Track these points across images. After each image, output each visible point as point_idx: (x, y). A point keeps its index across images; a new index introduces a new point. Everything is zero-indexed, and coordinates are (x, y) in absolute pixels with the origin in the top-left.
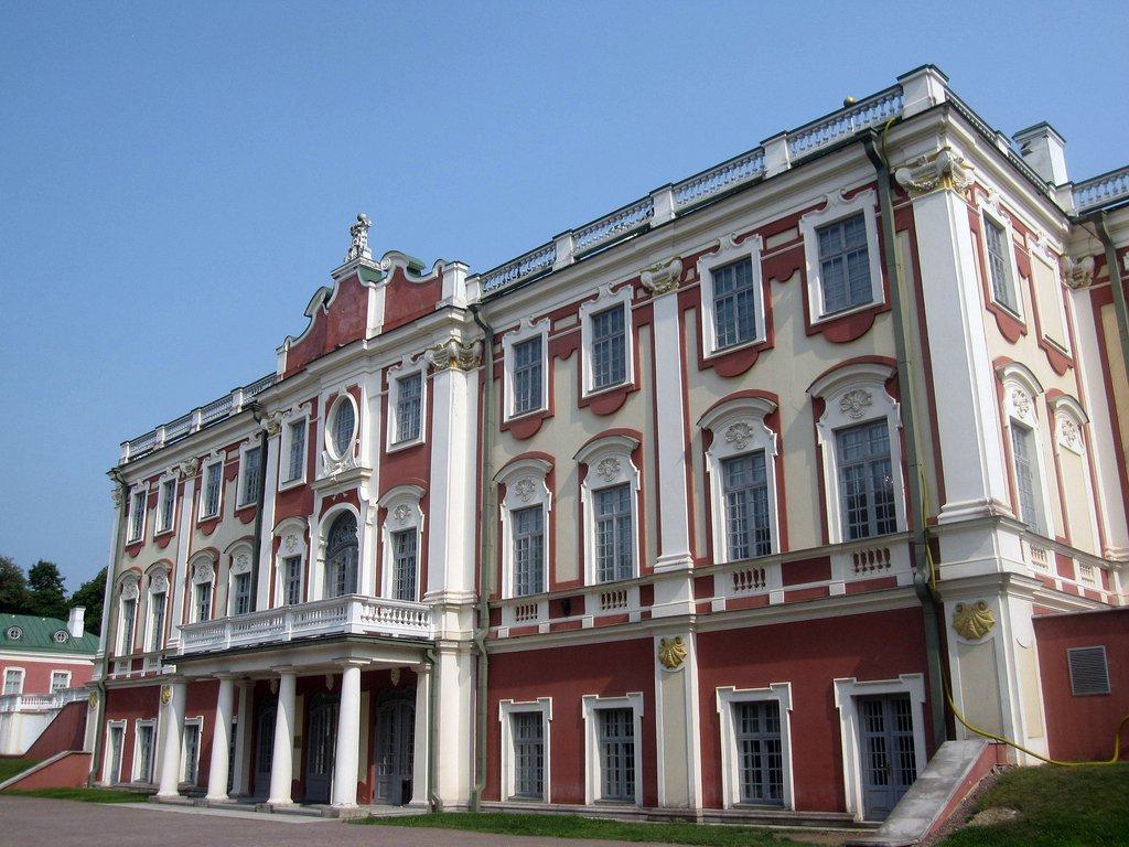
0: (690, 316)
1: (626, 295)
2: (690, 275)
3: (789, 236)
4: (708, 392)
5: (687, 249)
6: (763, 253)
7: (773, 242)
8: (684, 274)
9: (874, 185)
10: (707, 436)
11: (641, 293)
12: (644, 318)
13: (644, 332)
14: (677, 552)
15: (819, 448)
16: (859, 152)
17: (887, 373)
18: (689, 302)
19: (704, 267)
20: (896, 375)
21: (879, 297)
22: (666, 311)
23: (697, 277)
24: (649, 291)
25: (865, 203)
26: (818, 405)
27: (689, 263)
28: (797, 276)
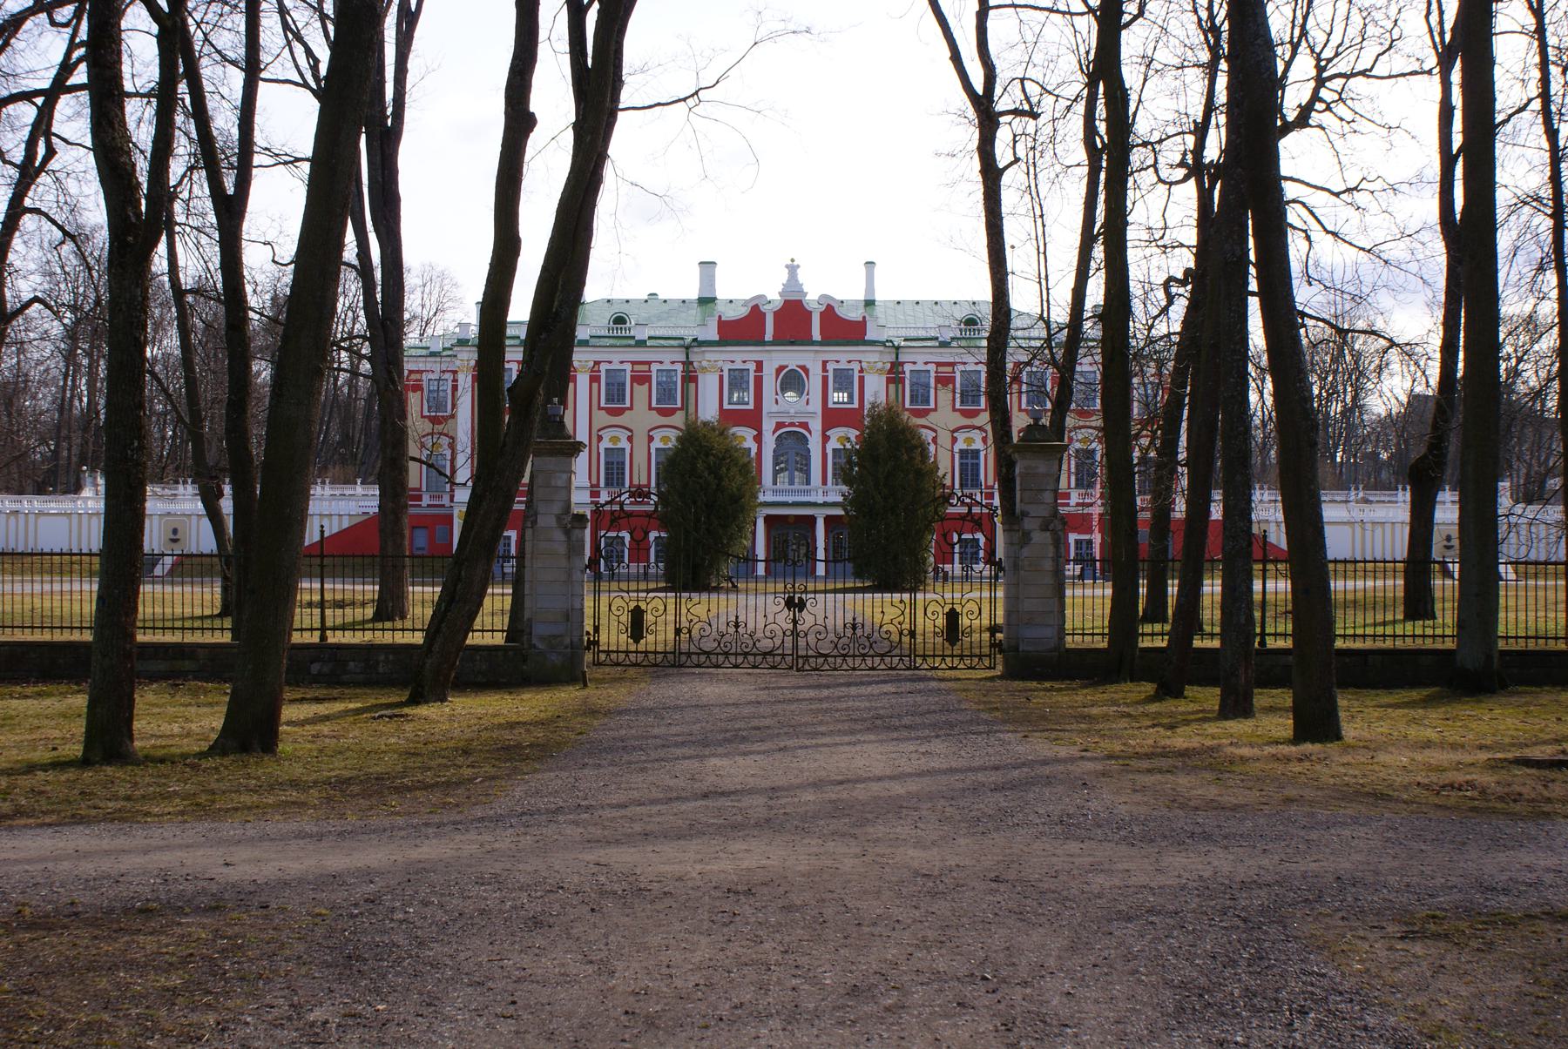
0: (595, 385)
3: (645, 368)
4: (602, 418)
5: (598, 357)
7: (637, 367)
10: (600, 438)
18: (594, 379)
19: (603, 367)
25: (679, 367)
26: (651, 439)
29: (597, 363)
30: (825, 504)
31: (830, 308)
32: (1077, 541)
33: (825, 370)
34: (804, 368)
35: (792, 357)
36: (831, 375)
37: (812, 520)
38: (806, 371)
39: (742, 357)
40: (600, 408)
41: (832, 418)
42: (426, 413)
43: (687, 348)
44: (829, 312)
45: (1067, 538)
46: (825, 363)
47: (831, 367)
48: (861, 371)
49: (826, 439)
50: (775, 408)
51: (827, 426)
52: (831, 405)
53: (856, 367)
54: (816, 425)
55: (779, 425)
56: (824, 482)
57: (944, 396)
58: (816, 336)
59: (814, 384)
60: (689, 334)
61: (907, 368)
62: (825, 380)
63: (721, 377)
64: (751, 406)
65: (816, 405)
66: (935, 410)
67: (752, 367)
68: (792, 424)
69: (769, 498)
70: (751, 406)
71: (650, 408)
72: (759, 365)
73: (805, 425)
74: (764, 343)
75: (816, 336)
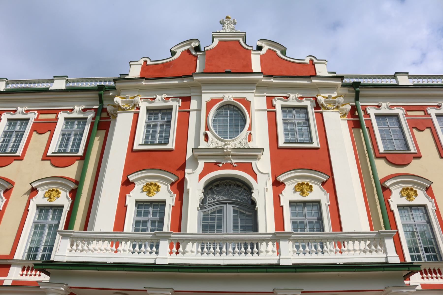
7: (42, 116)
9: (96, 110)
15: (27, 211)
16: (95, 95)
17: (73, 186)
20: (76, 189)
21: (81, 153)
26: (34, 191)
28: (48, 133)
33: (270, 105)
38: (247, 104)
46: (270, 100)
47: (278, 104)
49: (278, 185)
50: (203, 145)
54: (263, 164)
57: (424, 138)
59: (258, 121)
61: (372, 112)
63: (137, 115)
66: (418, 156)
70: (171, 145)
71: (45, 158)
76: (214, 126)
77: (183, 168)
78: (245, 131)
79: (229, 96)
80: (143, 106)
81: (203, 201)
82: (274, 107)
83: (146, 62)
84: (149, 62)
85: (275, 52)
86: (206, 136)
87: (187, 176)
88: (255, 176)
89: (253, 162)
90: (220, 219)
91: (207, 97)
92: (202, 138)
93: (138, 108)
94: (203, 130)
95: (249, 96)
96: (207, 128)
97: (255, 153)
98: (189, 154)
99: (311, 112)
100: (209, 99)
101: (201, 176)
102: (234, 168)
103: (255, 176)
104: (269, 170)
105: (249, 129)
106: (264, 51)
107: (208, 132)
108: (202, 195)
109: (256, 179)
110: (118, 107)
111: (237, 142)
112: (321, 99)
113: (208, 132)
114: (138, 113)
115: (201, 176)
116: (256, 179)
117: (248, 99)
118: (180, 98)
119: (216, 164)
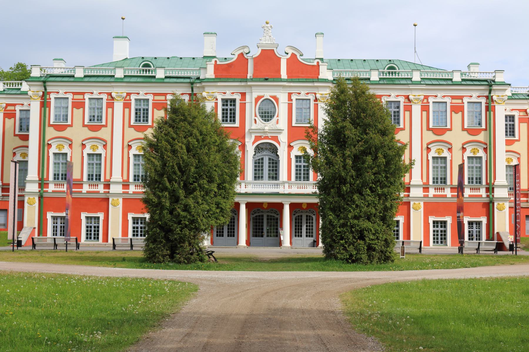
0: (127, 110)
1: (105, 97)
2: (128, 98)
6: (153, 100)
8: (126, 97)
10: (130, 147)
11: (110, 98)
12: (110, 105)
13: (110, 110)
14: (117, 176)
18: (127, 105)
19: (133, 97)
22: (118, 106)
23: (130, 100)
24: (113, 98)
27: (129, 94)
29: (129, 94)
30: (289, 195)
31: (293, 55)
32: (470, 223)
33: (290, 99)
34: (275, 98)
35: (267, 92)
36: (294, 102)
37: (281, 206)
38: (277, 100)
39: (230, 91)
40: (130, 126)
41: (294, 133)
42: (17, 133)
43: (192, 83)
44: (293, 61)
45: (448, 215)
46: (290, 94)
47: (294, 97)
48: (316, 100)
49: (290, 147)
50: (254, 126)
51: (292, 138)
52: (294, 125)
53: (311, 97)
54: (283, 138)
55: (257, 138)
56: (289, 178)
58: (284, 74)
60: (193, 74)
62: (290, 106)
63: (216, 104)
64: (237, 124)
65: (283, 125)
67: (238, 97)
68: (266, 138)
69: (250, 189)
70: (237, 124)
72: (243, 95)
73: (276, 139)
74: (246, 80)
75: (284, 74)
76: (259, 113)
77: (244, 137)
78: (275, 119)
79: (267, 95)
80: (220, 97)
81: (255, 155)
82: (292, 100)
83: (216, 61)
84: (218, 63)
85: (296, 55)
86: (255, 120)
87: (246, 143)
88: (279, 143)
89: (279, 136)
90: (262, 163)
91: (255, 95)
92: (253, 121)
93: (217, 99)
94: (253, 117)
95: (278, 95)
96: (256, 116)
97: (280, 131)
98: (247, 130)
99: (312, 103)
100: (256, 96)
101: (253, 143)
102: (269, 139)
103: (279, 143)
104: (286, 141)
105: (278, 116)
106: (289, 56)
107: (256, 118)
108: (254, 153)
109: (280, 145)
110: (205, 98)
111: (270, 124)
112: (318, 96)
113: (256, 118)
114: (217, 103)
115: (253, 143)
116: (280, 145)
117: (278, 96)
118: (240, 93)
119: (261, 136)
